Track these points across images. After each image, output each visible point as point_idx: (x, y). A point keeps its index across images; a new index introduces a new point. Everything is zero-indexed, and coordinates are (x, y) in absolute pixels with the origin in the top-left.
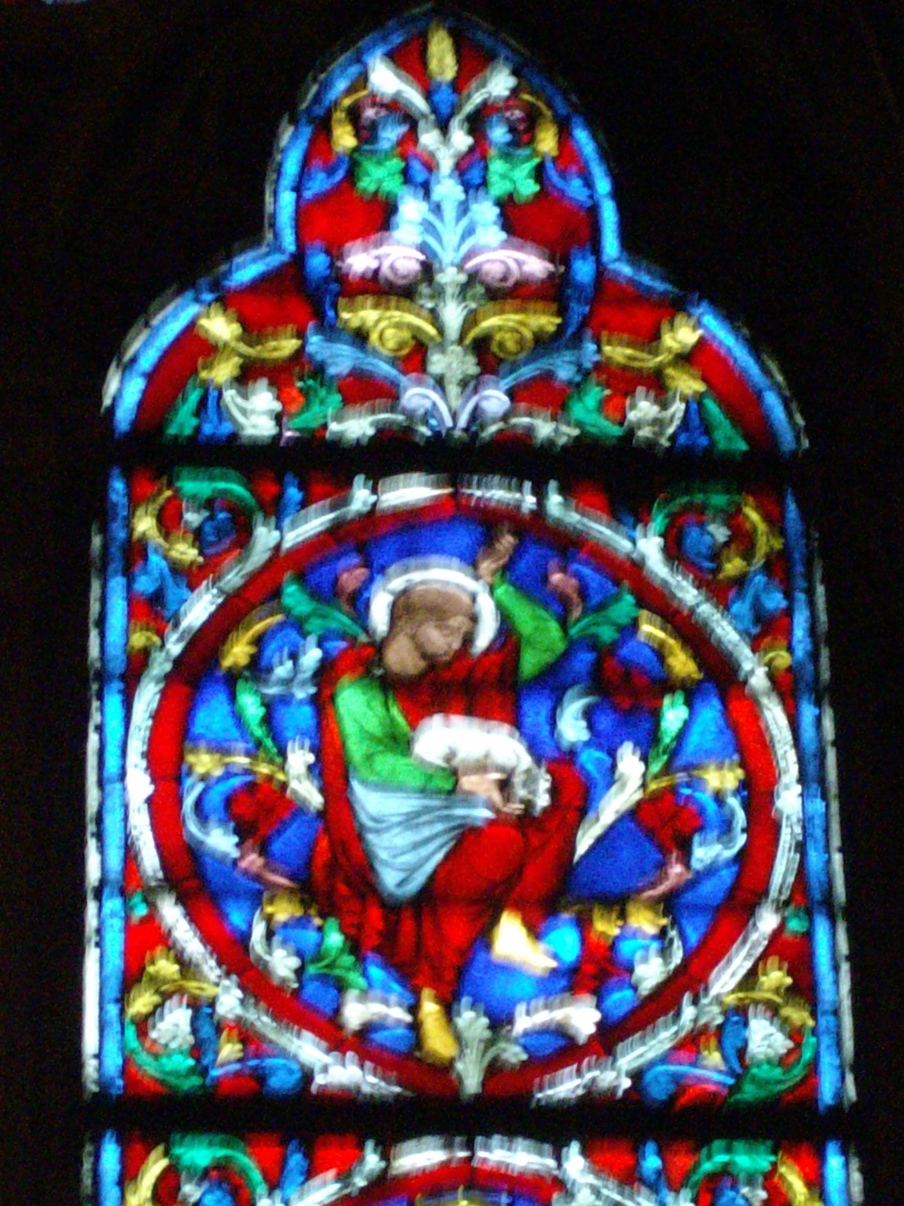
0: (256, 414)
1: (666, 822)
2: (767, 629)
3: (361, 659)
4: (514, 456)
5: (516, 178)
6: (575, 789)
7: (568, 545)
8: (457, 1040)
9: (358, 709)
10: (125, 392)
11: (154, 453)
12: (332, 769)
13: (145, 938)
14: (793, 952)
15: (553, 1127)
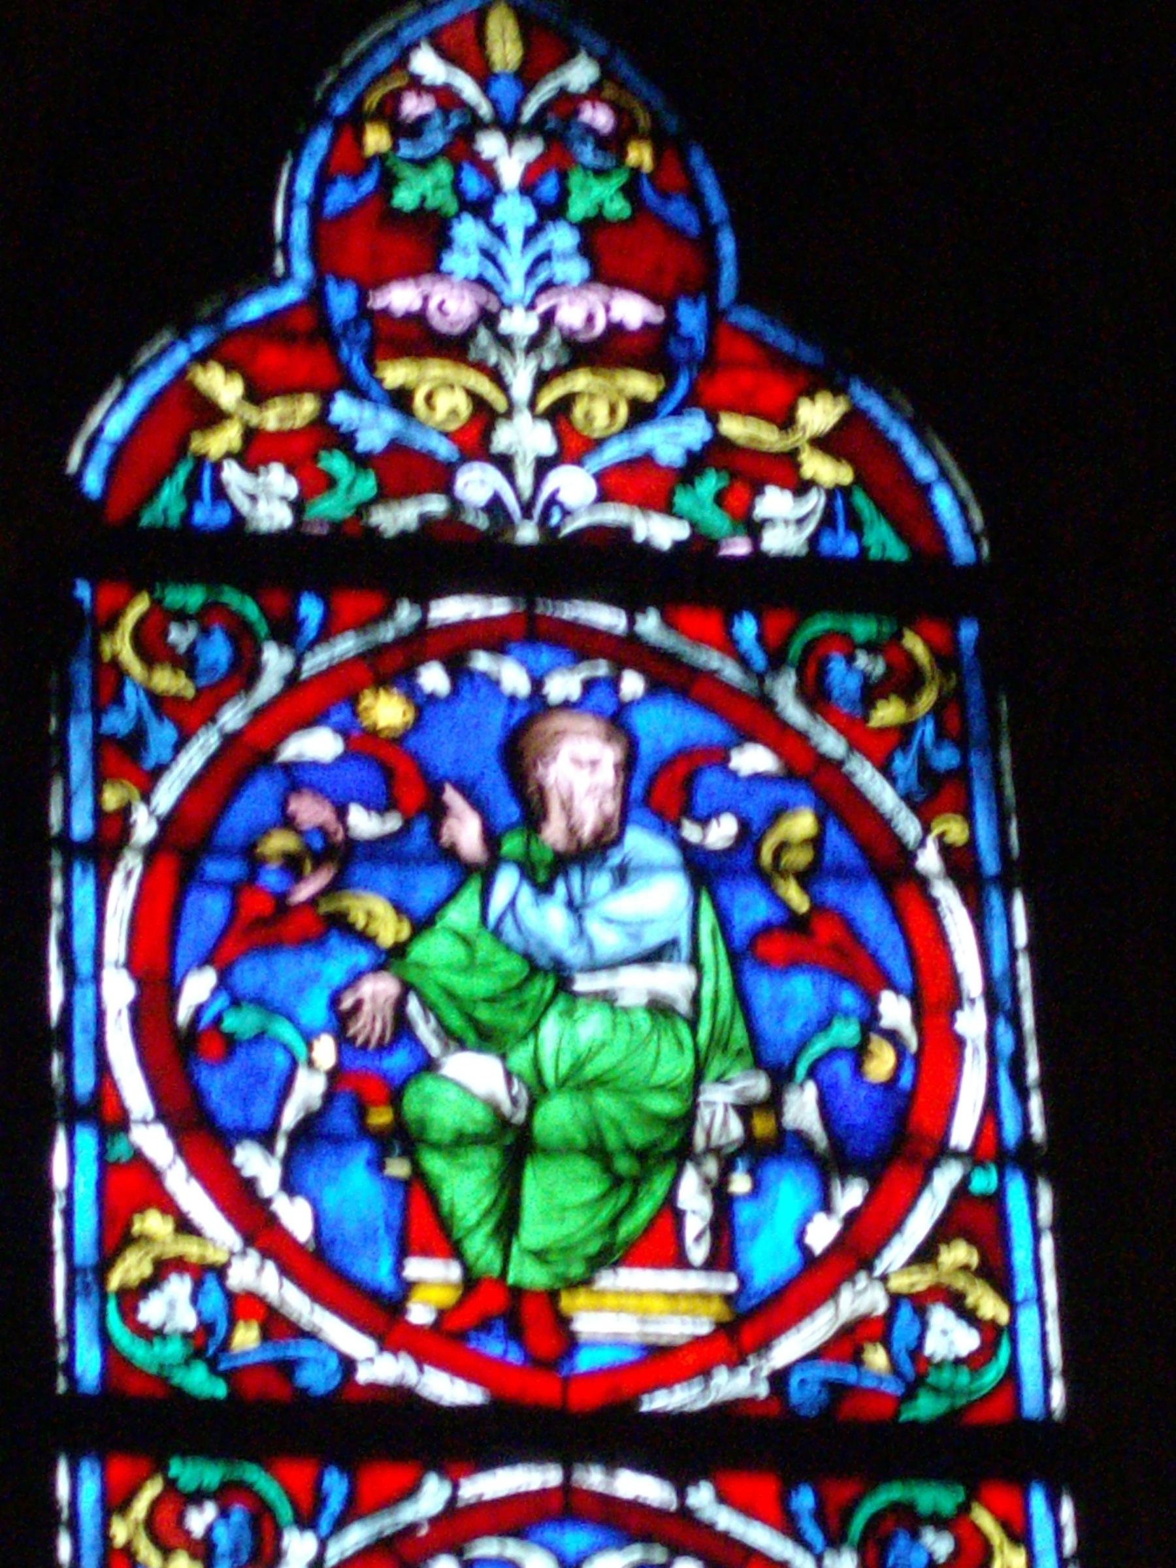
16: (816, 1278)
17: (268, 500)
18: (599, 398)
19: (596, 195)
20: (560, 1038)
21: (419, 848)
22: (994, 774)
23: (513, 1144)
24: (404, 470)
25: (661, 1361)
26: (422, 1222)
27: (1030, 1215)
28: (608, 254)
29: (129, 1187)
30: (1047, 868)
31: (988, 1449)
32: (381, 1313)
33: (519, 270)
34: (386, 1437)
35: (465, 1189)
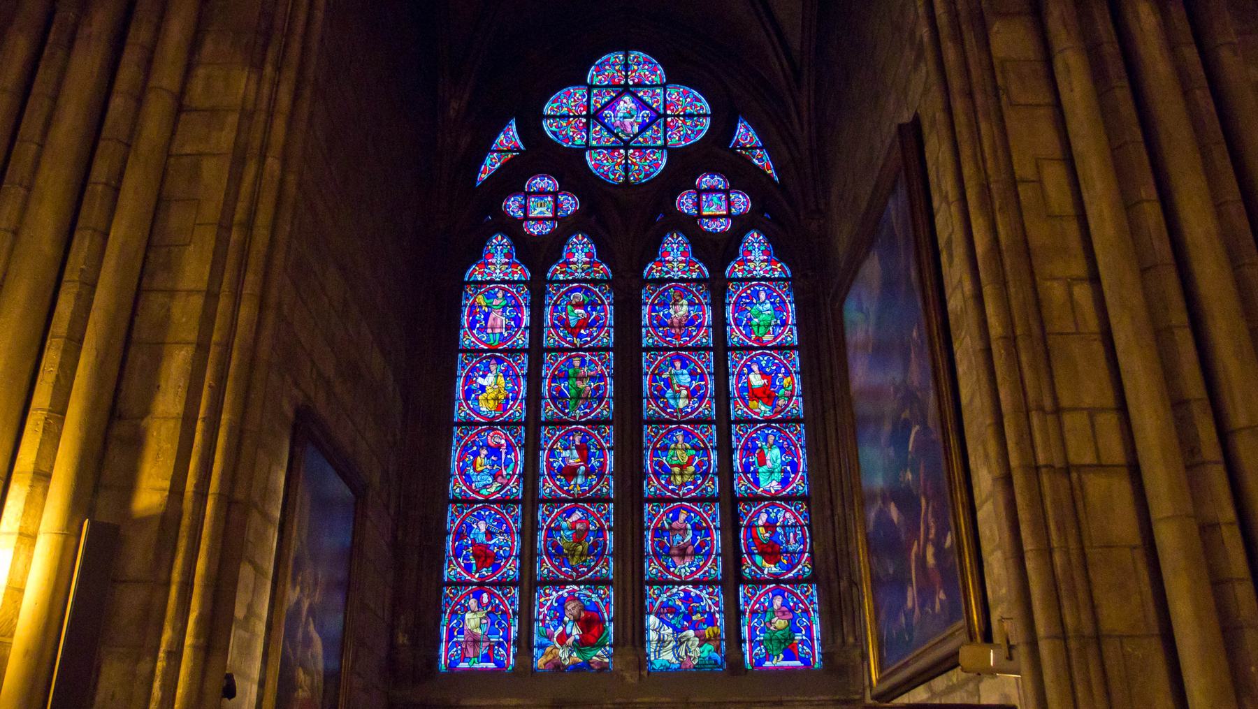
0: (561, 277)
1: (596, 320)
2: (608, 298)
3: (569, 303)
4: (585, 281)
5: (586, 250)
6: (590, 315)
7: (590, 290)
8: (577, 341)
9: (569, 307)
10: (549, 275)
11: (551, 282)
12: (567, 315)
13: (550, 332)
14: (608, 332)
15: (585, 350)
16: (780, 335)
17: (740, 275)
18: (763, 265)
19: (763, 248)
20: (762, 317)
21: (751, 304)
22: (792, 294)
23: (759, 325)
24: (750, 272)
25: (769, 342)
26: (752, 332)
27: (795, 329)
28: (764, 253)
29: (732, 330)
30: (796, 302)
31: (792, 348)
32: (750, 339)
33: (757, 255)
34: (751, 348)
35: (755, 329)
